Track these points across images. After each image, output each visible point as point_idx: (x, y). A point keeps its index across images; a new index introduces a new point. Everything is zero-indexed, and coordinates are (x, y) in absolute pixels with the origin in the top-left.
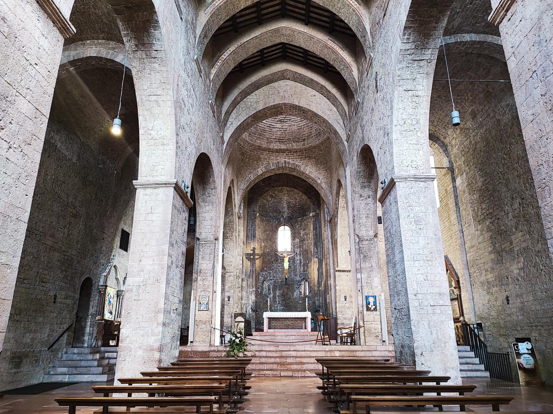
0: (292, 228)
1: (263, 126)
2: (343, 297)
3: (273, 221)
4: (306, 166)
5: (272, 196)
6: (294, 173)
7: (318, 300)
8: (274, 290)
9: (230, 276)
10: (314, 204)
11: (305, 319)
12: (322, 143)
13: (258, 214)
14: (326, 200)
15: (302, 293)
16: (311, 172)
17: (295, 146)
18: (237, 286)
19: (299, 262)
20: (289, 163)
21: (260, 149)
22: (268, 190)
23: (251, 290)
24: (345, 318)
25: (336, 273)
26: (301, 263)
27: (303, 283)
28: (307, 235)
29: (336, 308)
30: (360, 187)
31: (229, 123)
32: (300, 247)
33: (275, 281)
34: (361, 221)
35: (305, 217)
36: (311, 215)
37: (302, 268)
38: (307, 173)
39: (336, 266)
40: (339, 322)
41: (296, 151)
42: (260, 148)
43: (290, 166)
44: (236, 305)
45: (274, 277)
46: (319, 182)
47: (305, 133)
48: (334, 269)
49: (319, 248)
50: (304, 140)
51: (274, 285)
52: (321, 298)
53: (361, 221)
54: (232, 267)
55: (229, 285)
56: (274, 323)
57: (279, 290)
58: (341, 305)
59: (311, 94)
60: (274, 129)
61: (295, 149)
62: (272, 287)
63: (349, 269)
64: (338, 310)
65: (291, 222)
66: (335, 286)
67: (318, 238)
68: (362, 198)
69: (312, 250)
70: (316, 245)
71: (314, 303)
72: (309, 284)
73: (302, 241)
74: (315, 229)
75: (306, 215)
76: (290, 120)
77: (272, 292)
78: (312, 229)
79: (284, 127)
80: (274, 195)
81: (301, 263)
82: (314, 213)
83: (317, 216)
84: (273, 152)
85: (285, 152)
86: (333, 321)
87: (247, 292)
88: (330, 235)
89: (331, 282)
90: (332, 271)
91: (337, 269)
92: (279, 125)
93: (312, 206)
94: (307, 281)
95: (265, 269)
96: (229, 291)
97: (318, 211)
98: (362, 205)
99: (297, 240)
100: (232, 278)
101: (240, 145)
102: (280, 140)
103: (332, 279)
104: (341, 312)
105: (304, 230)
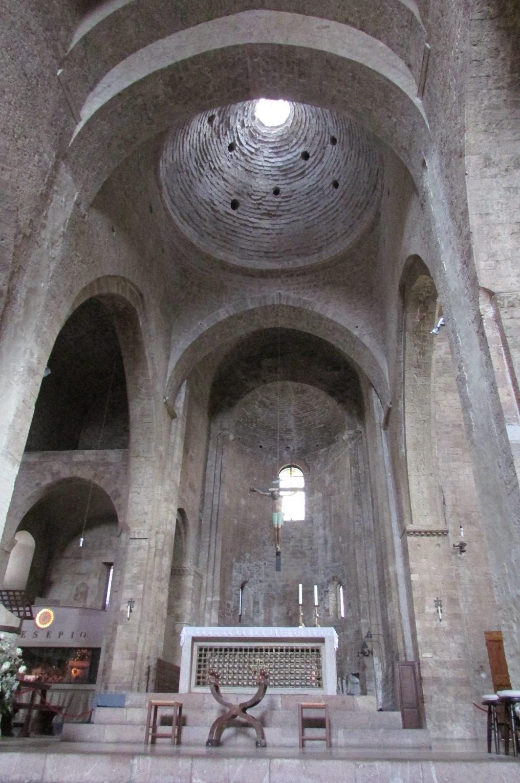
0: (307, 470)
1: (231, 222)
2: (430, 600)
3: (266, 454)
4: (327, 303)
5: (262, 404)
6: (302, 326)
7: (366, 624)
8: (268, 605)
9: (139, 548)
10: (350, 413)
11: (312, 650)
12: (359, 244)
13: (231, 437)
14: (374, 379)
15: (331, 612)
16: (338, 316)
17: (300, 263)
18: (156, 574)
19: (321, 541)
20: (288, 297)
21: (224, 269)
22: (253, 388)
23: (209, 599)
24: (442, 664)
25: (409, 539)
26: (326, 542)
27: (331, 588)
28: (338, 483)
29: (414, 636)
30: (481, 127)
31: (99, 88)
32: (324, 508)
33: (270, 586)
34: (495, 247)
35: (333, 446)
36: (345, 437)
37: (329, 554)
38: (329, 315)
39: (407, 521)
40: (425, 673)
41: (302, 272)
42: (223, 266)
43: (290, 304)
44: (150, 625)
45: (267, 576)
46: (356, 333)
47: (321, 234)
48: (404, 533)
49: (365, 505)
50: (320, 249)
51: (267, 595)
52: (374, 621)
53: (495, 247)
54: (147, 527)
55: (135, 570)
56: (214, 662)
57: (280, 604)
58: (427, 625)
59: (318, 25)
60: (254, 232)
61: (300, 269)
62: (261, 598)
63: (441, 527)
64: (419, 638)
65: (302, 459)
66: (408, 572)
67: (363, 484)
68: (494, 170)
69: (351, 512)
70: (357, 497)
71: (358, 632)
72: (344, 589)
73: (328, 495)
74: (355, 464)
75: (334, 441)
76: (288, 210)
77: (262, 611)
78: (348, 466)
79: (277, 227)
80: (268, 402)
81: (326, 542)
82: (351, 432)
83: (358, 437)
84: (253, 276)
85: (279, 277)
86: (408, 671)
87: (197, 603)
88: (387, 455)
89: (397, 567)
90: (396, 532)
91: (410, 527)
92: (266, 223)
93: (347, 419)
94: (340, 583)
95: (248, 556)
96: (132, 587)
97: (359, 428)
98: (496, 194)
99: (319, 495)
100: (142, 554)
101: (177, 250)
102: (267, 254)
103: (399, 560)
104: (430, 645)
105: (332, 471)
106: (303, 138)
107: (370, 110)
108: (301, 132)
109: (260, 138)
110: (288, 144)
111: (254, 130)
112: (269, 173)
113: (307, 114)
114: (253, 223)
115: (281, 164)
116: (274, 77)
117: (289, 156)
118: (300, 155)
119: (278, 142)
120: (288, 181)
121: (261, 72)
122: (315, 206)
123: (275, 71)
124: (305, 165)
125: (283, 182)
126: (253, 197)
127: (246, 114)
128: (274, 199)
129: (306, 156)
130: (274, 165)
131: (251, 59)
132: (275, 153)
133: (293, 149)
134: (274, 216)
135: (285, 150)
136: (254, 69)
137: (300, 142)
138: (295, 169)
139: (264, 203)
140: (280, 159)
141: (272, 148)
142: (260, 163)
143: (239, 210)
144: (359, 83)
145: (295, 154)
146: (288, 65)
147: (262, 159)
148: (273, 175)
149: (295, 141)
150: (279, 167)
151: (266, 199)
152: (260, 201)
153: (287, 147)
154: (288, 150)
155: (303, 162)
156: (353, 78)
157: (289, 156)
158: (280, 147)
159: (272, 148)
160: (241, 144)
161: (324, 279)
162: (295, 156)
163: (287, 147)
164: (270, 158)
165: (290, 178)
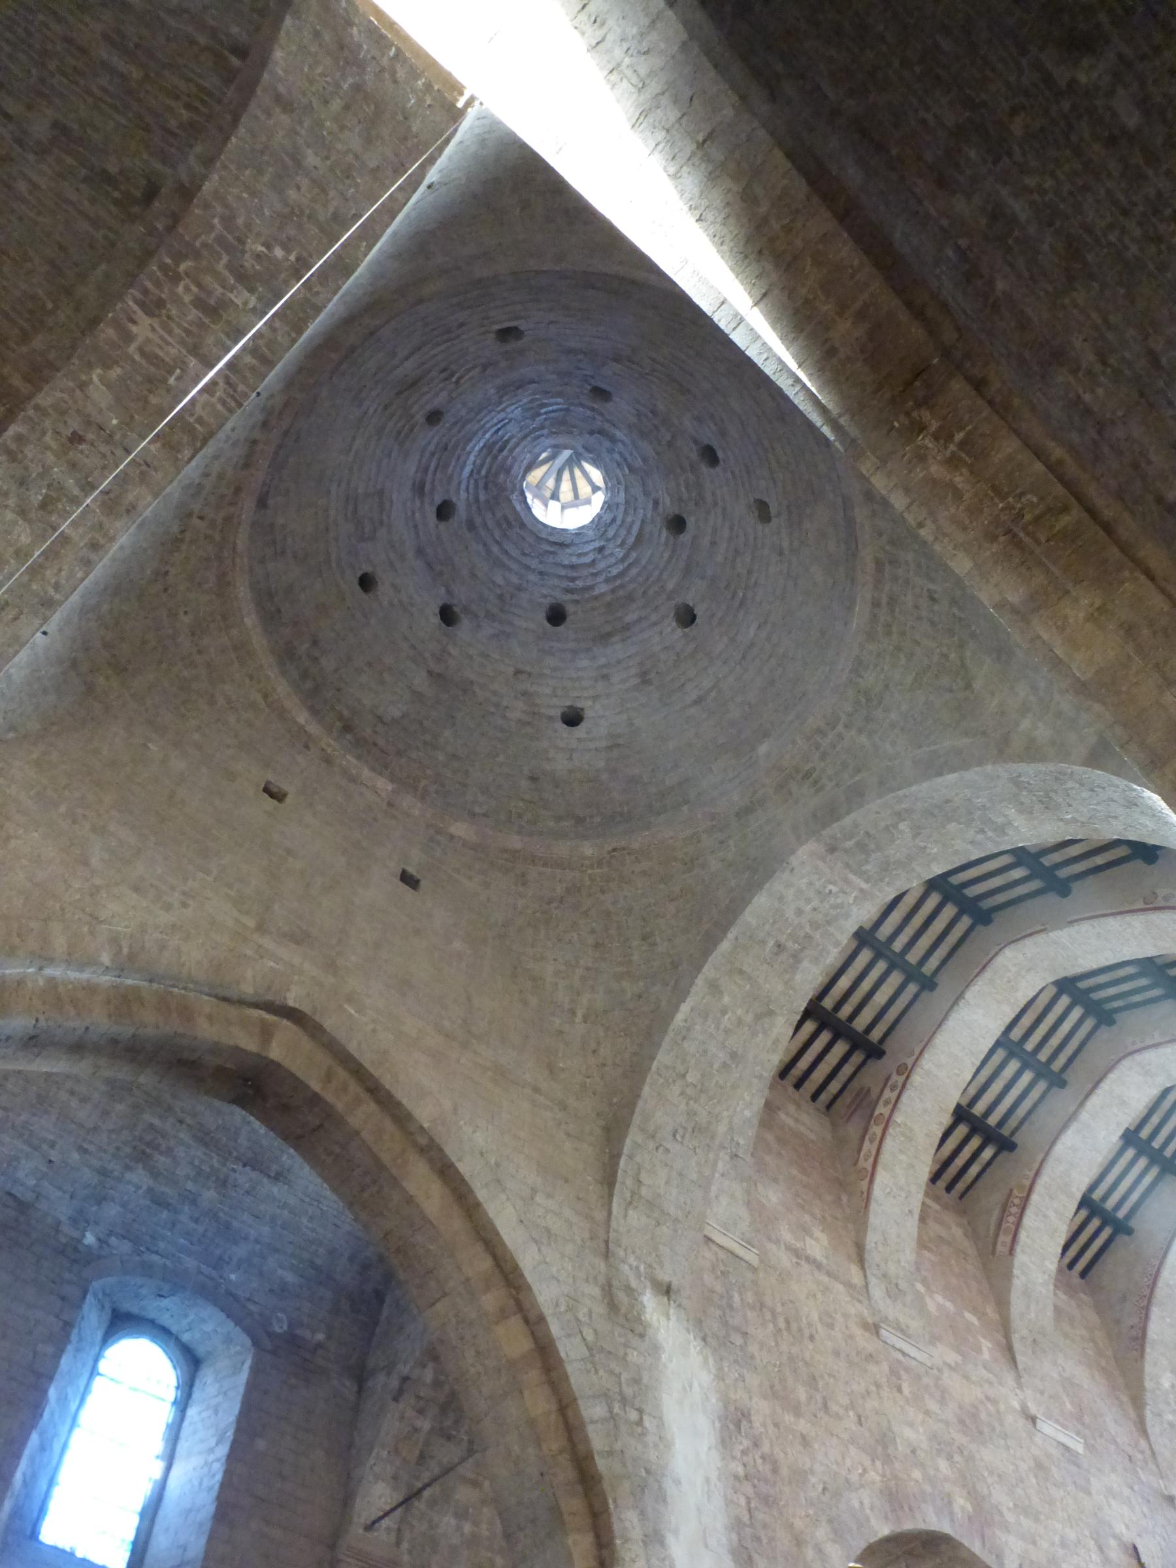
106: (478, 521)
107: (684, 1076)
108: (490, 524)
109: (545, 431)
110: (486, 476)
111: (571, 433)
112: (479, 417)
113: (514, 566)
114: (438, 344)
115: (468, 448)
116: (808, 901)
117: (468, 470)
118: (454, 500)
119: (507, 457)
120: (432, 448)
121: (831, 887)
122: (351, 507)
123: (815, 909)
124: (431, 504)
125: (435, 441)
126: (478, 370)
127: (617, 457)
128: (428, 408)
129: (444, 511)
130: (480, 433)
131: (862, 890)
132: (495, 443)
133: (471, 486)
134: (399, 393)
135: (482, 466)
136: (846, 880)
137: (474, 508)
138: (438, 475)
139: (441, 385)
140: (477, 448)
141: (507, 441)
142: (509, 410)
143: (493, 336)
144: (725, 1065)
145: (463, 486)
146: (808, 937)
147: (510, 416)
148: (469, 421)
149: (482, 498)
150: (470, 440)
151: (444, 394)
152: (454, 379)
153: (483, 472)
154: (479, 472)
155: (438, 500)
156: (733, 1055)
157: (468, 470)
158: (496, 457)
159: (507, 441)
160: (581, 405)
161: (201, 518)
162: (460, 483)
163: (483, 472)
164: (499, 429)
165: (433, 454)
